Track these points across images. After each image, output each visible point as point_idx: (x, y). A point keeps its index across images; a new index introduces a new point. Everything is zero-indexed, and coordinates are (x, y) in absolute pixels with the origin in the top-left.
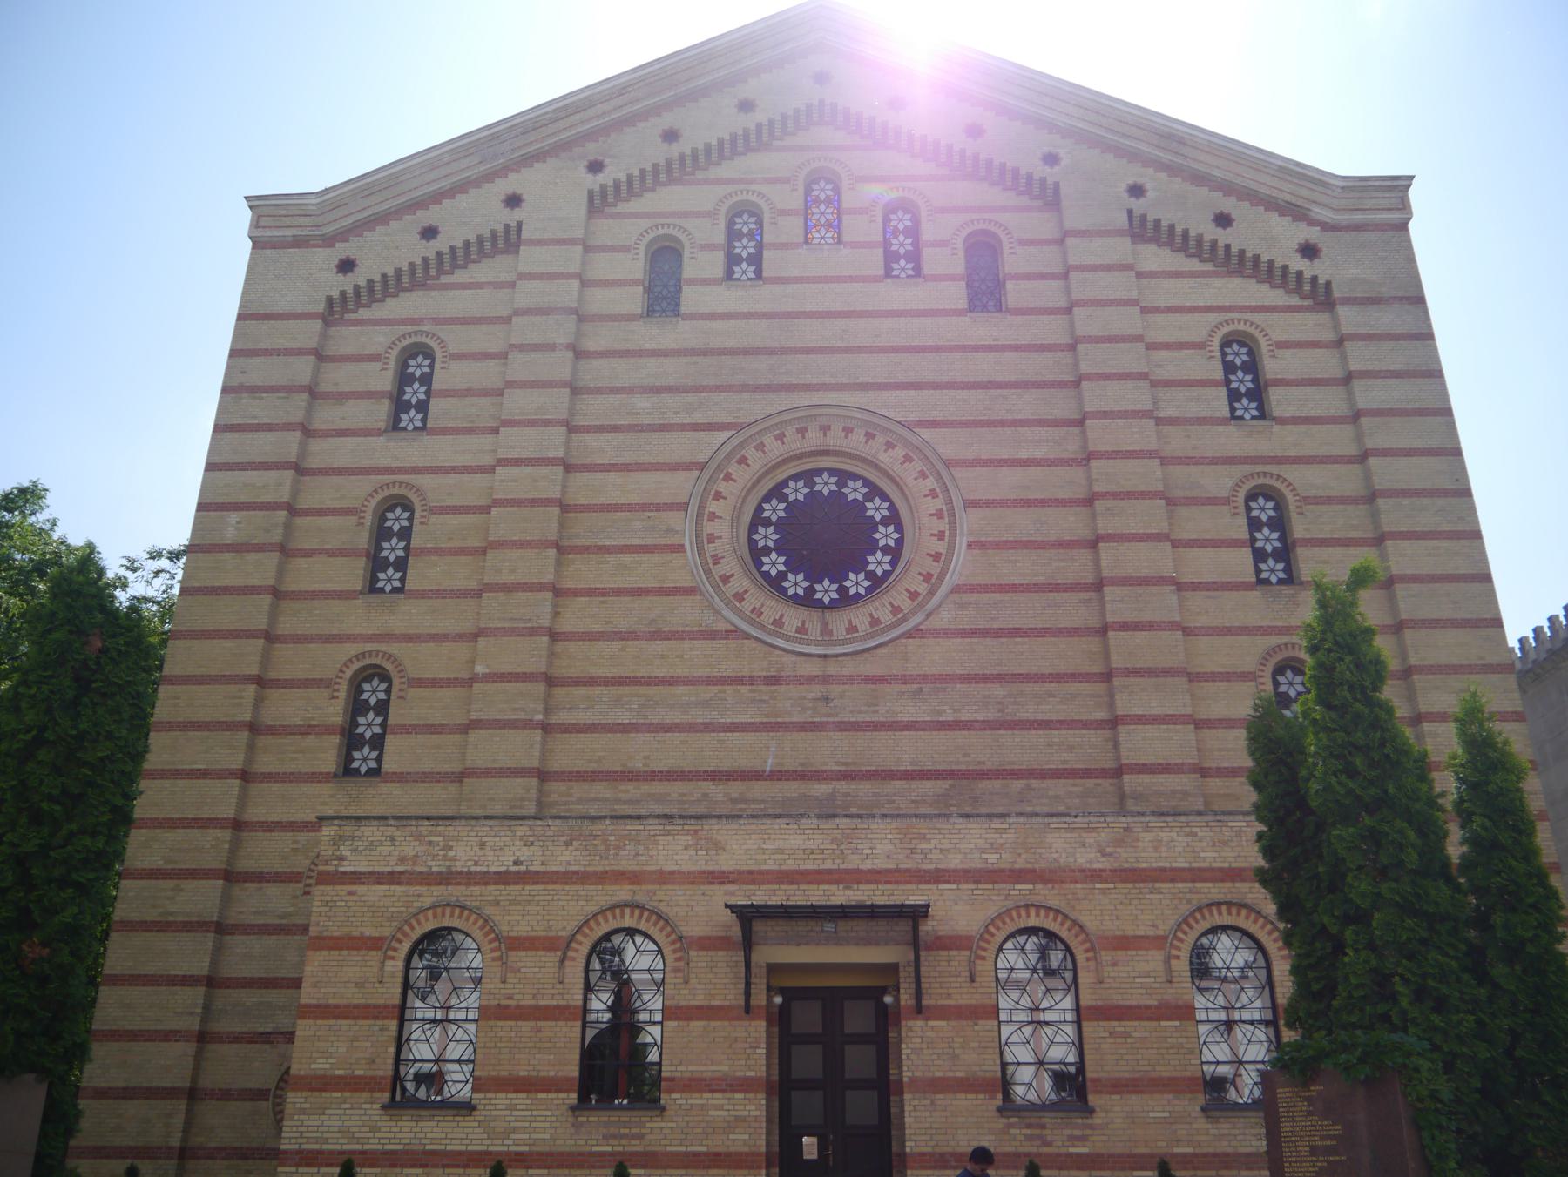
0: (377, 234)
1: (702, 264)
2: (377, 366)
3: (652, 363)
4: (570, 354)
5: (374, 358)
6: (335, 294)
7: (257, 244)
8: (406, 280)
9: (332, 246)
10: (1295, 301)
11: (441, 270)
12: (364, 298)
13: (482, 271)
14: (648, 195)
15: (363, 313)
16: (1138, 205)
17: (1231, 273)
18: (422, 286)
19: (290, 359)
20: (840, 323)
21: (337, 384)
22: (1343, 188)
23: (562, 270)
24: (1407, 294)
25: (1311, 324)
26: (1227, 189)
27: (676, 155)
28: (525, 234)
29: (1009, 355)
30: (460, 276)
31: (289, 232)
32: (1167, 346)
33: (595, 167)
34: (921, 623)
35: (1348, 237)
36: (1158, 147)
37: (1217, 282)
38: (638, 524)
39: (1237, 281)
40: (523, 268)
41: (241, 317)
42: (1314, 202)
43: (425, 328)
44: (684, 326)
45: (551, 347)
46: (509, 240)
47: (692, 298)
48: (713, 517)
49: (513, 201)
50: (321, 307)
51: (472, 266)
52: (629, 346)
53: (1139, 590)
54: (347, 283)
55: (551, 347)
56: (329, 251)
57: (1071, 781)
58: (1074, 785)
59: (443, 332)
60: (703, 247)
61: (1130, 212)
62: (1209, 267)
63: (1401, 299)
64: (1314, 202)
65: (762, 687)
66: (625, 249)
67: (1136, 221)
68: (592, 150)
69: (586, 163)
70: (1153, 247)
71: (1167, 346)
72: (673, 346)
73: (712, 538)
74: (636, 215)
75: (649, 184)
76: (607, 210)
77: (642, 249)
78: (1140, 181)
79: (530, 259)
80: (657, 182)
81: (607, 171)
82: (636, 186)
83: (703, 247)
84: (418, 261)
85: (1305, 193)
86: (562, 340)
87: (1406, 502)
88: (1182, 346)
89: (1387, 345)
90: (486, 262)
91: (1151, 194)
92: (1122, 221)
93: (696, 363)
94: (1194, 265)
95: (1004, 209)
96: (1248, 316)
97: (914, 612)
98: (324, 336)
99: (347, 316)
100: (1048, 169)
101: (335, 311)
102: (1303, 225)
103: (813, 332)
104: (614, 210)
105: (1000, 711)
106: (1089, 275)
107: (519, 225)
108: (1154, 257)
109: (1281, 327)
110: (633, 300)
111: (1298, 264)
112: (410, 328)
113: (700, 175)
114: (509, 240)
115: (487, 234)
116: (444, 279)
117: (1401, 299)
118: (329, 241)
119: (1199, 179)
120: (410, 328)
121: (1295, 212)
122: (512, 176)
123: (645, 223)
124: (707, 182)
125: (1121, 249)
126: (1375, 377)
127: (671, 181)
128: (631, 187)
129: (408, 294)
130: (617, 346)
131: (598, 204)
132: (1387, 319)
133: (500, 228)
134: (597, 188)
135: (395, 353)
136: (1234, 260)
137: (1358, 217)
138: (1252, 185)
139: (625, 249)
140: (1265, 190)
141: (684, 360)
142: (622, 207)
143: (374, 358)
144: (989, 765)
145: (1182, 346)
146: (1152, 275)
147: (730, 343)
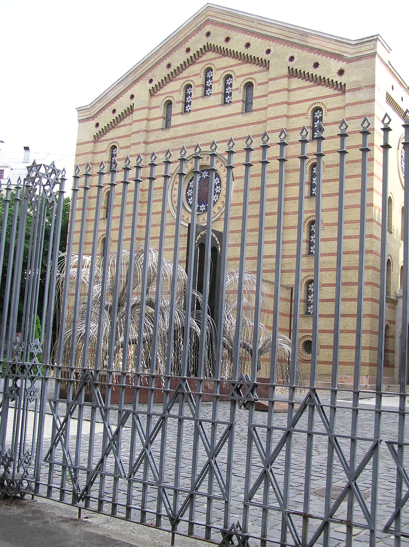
0: (103, 114)
1: (177, 108)
2: (105, 153)
3: (164, 143)
4: (143, 145)
5: (104, 151)
6: (95, 135)
7: (80, 121)
8: (110, 127)
9: (94, 120)
10: (336, 92)
11: (118, 122)
12: (102, 134)
13: (127, 121)
14: (164, 87)
15: (103, 138)
16: (292, 65)
17: (319, 84)
18: (113, 128)
19: (87, 155)
20: (208, 123)
21: (97, 160)
22: (355, 44)
23: (142, 118)
24: (369, 84)
25: (337, 101)
26: (319, 51)
27: (170, 73)
28: (135, 108)
29: (251, 126)
30: (122, 123)
31: (85, 117)
32: (295, 116)
33: (151, 81)
34: (220, 216)
35: (354, 64)
36: (299, 40)
37: (314, 89)
38: (158, 193)
39: (320, 87)
40: (134, 119)
41: (77, 145)
42: (345, 52)
43: (115, 141)
44: (171, 129)
45: (139, 143)
46: (131, 110)
47: (175, 120)
48: (175, 189)
49: (132, 97)
50: (92, 139)
51: (124, 119)
52: (159, 139)
53: (272, 202)
54: (97, 130)
55: (139, 143)
56: (93, 121)
57: (251, 261)
58: (251, 262)
59: (119, 141)
60: (177, 102)
61: (289, 67)
62: (312, 83)
63: (366, 87)
64: (345, 52)
65: (183, 238)
66: (158, 107)
67: (291, 71)
68: (149, 76)
69: (149, 80)
70: (296, 78)
71: (295, 116)
72: (169, 137)
73: (174, 196)
74: (162, 95)
75: (165, 83)
76: (155, 94)
77: (163, 106)
78: (293, 55)
79: (136, 115)
80: (167, 83)
81: (153, 82)
82: (161, 85)
83: (177, 102)
84: (112, 121)
85: (343, 49)
86: (142, 141)
87: (352, 165)
88: (299, 115)
89: (358, 106)
90: (128, 117)
91: (295, 60)
92: (286, 72)
93: (173, 142)
94: (308, 83)
95: (255, 73)
96: (321, 101)
97: (218, 213)
98: (95, 147)
99: (99, 140)
100: (267, 56)
101: (97, 138)
102: (341, 62)
103: (202, 127)
104: (157, 94)
105: (236, 241)
106: (273, 95)
107: (133, 104)
108: (296, 83)
109: (329, 103)
110: (160, 123)
111: (337, 79)
112: (112, 141)
113: (177, 77)
114: (131, 110)
115: (126, 109)
116: (119, 124)
117: (366, 87)
118: (93, 118)
119: (312, 49)
120: (112, 141)
121: (338, 57)
122: (132, 88)
123: (163, 97)
124: (179, 79)
125: (284, 83)
126: (352, 119)
127: (171, 81)
128: (160, 86)
129: (111, 131)
130: (156, 139)
131: (153, 93)
132: (361, 96)
133: (129, 107)
134: (151, 89)
135: (109, 149)
136: (318, 80)
137: (359, 55)
138: (326, 49)
139: (158, 107)
140: (330, 50)
141: (171, 141)
142: (159, 93)
143: (104, 151)
144: (232, 257)
145: (299, 115)
146: (295, 90)
147: (182, 134)
